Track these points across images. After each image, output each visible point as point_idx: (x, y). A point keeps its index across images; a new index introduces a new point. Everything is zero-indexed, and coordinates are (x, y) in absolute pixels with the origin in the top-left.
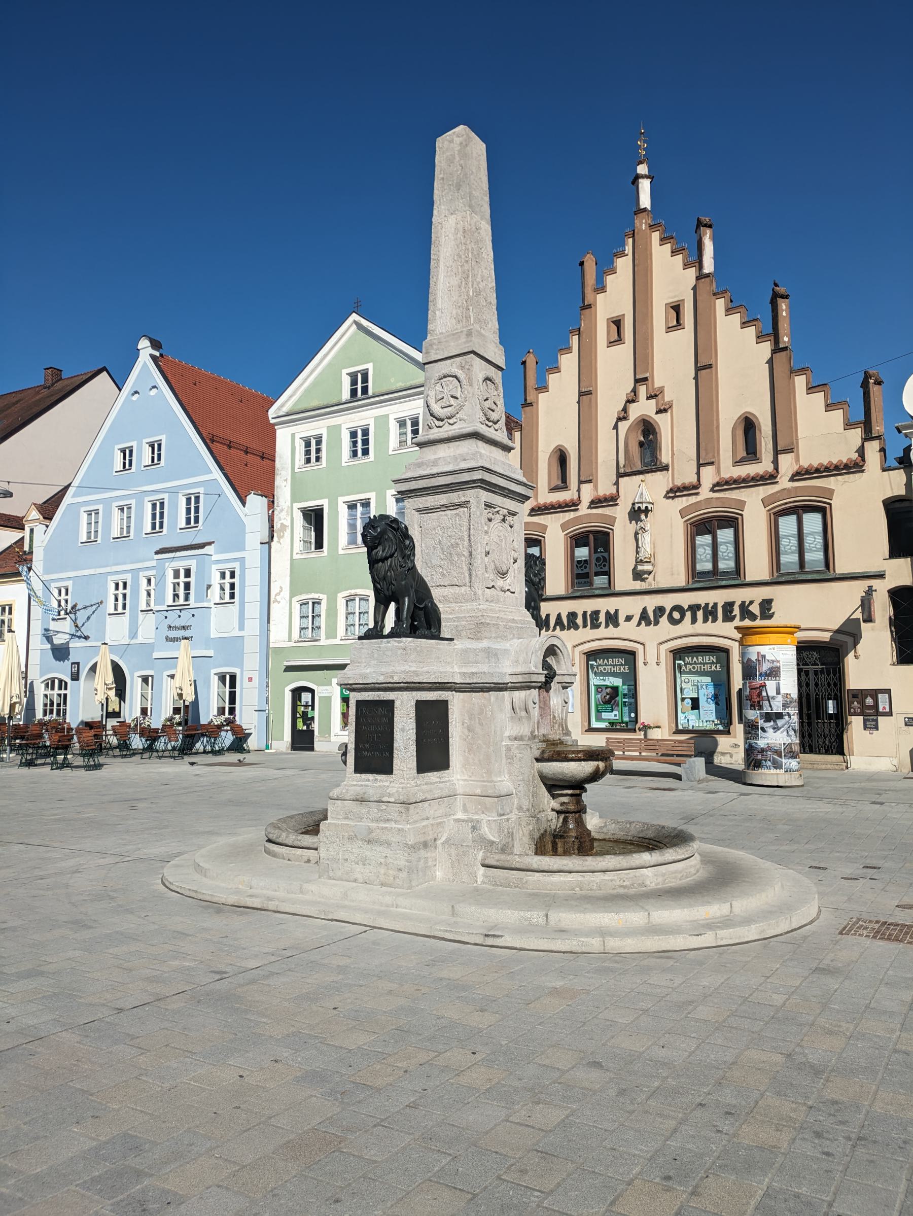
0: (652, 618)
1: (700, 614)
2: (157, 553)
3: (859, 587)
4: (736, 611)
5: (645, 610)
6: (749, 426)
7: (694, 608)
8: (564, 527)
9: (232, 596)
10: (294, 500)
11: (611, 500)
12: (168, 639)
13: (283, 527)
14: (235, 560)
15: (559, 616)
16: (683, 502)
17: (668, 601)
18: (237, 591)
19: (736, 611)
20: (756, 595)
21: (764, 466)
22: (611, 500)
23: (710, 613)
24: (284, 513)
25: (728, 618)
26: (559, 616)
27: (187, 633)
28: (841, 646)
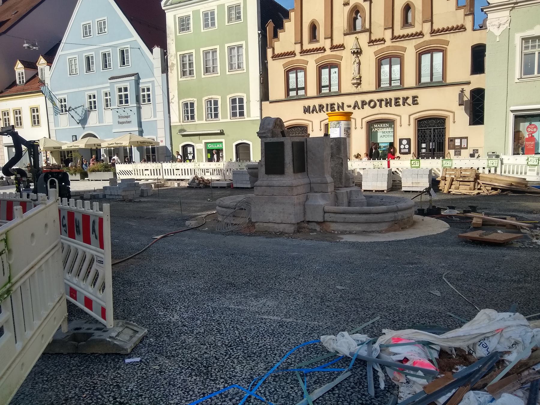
0: (360, 106)
1: (383, 103)
2: (110, 79)
3: (458, 89)
4: (401, 101)
5: (356, 102)
7: (381, 101)
9: (149, 100)
10: (177, 50)
11: (342, 47)
12: (119, 123)
13: (173, 64)
14: (149, 82)
15: (314, 106)
16: (376, 48)
17: (367, 98)
18: (151, 98)
19: (401, 101)
20: (410, 94)
21: (416, 29)
22: (342, 47)
23: (388, 103)
24: (173, 57)
25: (397, 104)
26: (314, 106)
27: (128, 120)
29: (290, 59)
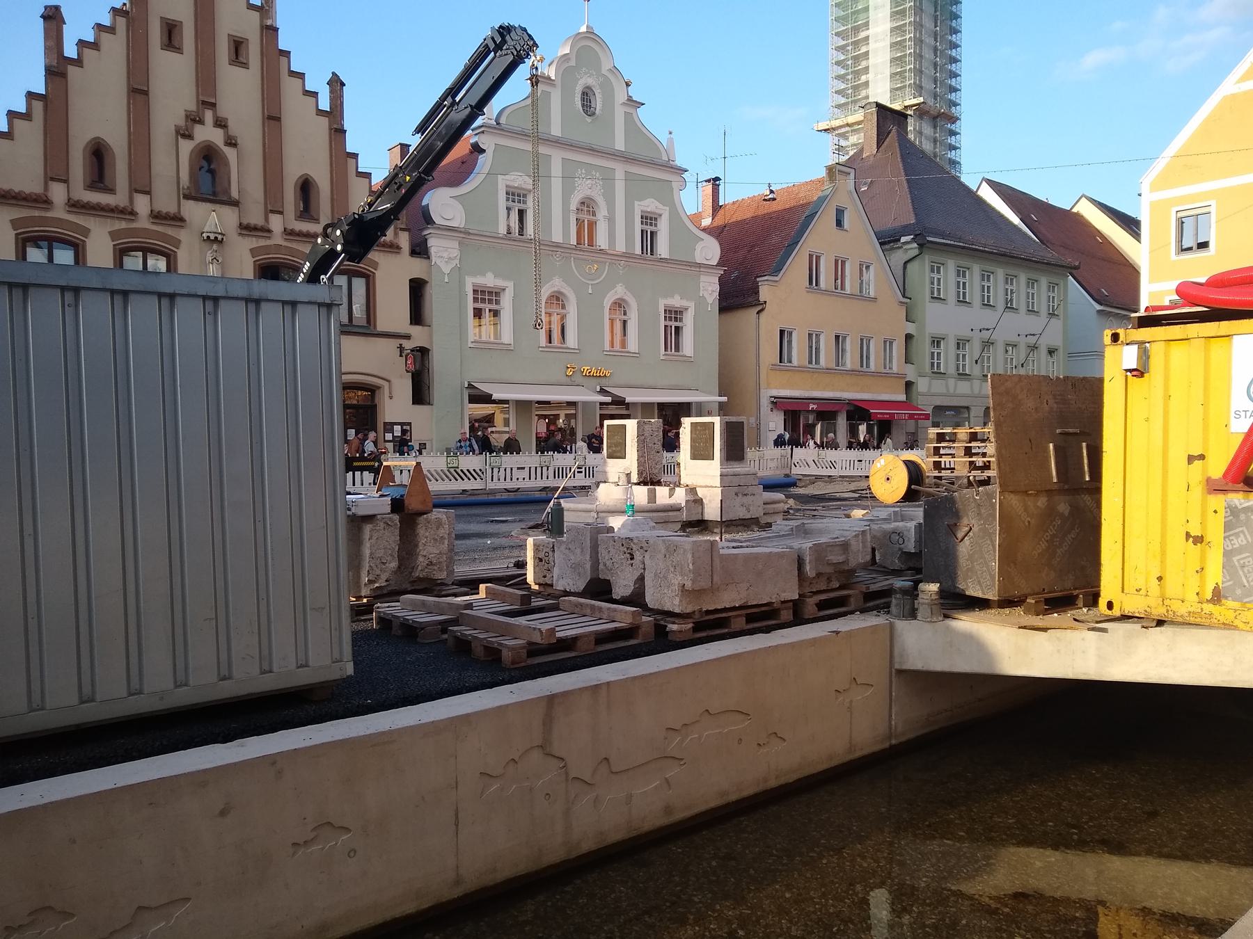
6: (306, 187)
8: (114, 235)
16: (254, 242)
28: (379, 388)
29: (36, 213)
